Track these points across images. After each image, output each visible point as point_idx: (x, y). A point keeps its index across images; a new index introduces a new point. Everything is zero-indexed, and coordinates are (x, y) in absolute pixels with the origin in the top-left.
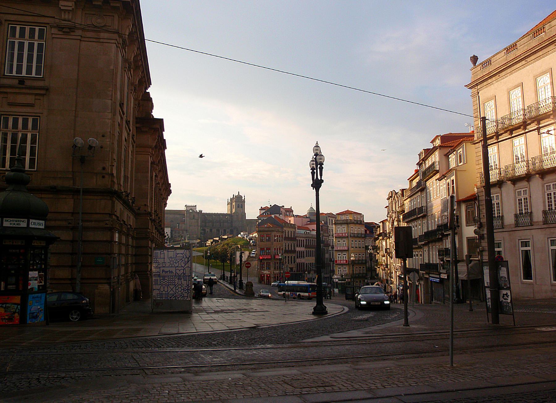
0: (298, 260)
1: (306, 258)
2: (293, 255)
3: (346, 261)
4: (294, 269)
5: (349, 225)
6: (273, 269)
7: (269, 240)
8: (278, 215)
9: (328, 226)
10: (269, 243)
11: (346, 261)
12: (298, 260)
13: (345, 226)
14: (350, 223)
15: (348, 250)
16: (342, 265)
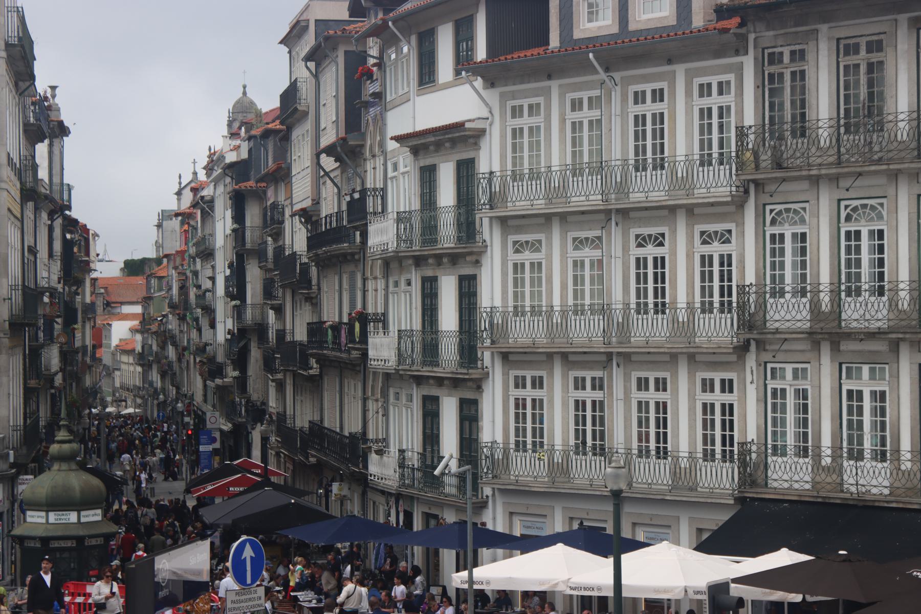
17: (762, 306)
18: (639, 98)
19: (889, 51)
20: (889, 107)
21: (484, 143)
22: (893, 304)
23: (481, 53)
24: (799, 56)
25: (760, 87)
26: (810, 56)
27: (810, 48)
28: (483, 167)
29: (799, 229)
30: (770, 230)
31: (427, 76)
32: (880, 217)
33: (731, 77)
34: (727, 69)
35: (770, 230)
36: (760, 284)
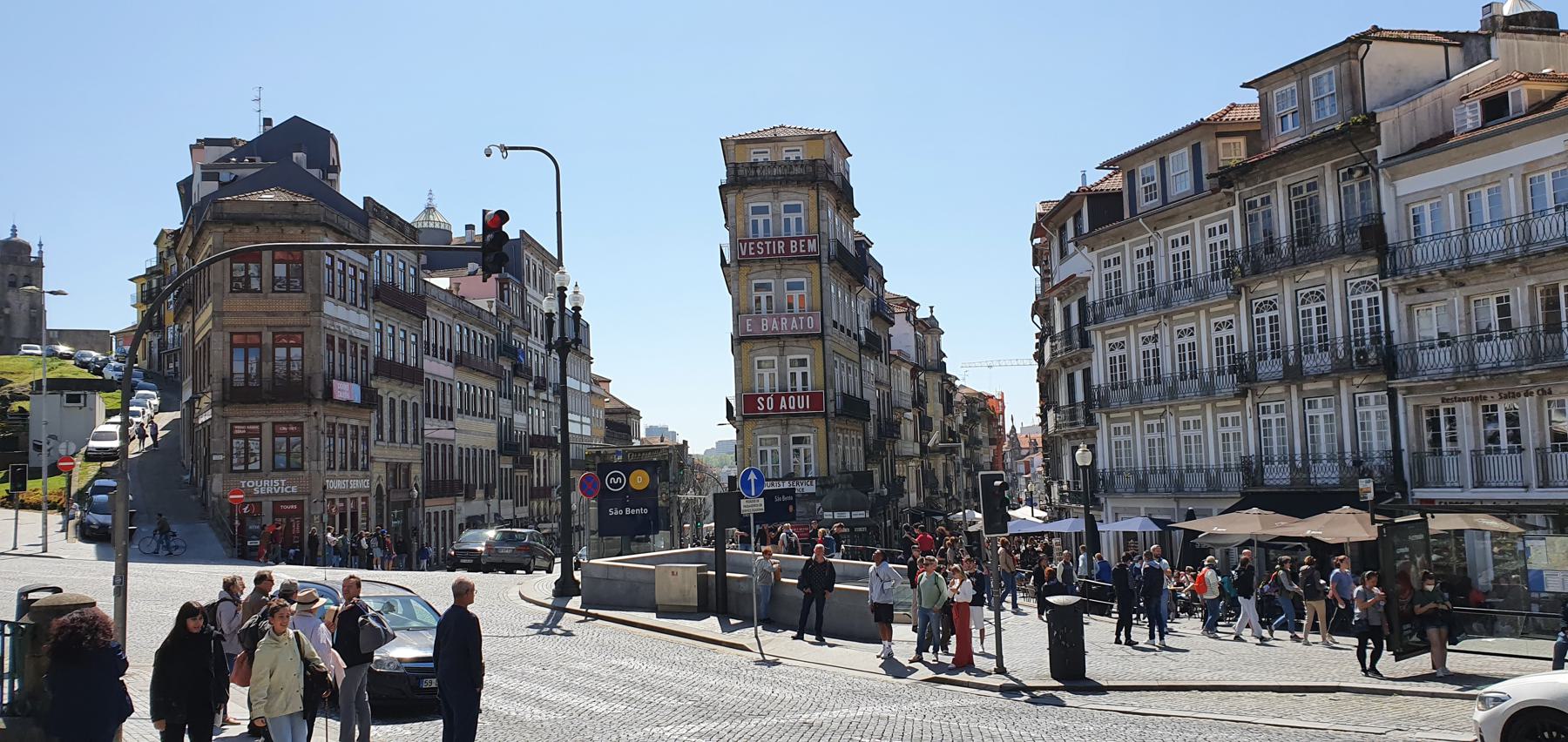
0: (435, 430)
1: (459, 421)
2: (412, 395)
3: (816, 399)
4: (416, 471)
5: (826, 195)
6: (323, 464)
7: (287, 286)
8: (315, 172)
9: (523, 290)
10: (295, 302)
11: (816, 399)
12: (435, 430)
13: (801, 197)
14: (831, 185)
15: (821, 336)
16: (786, 418)
17: (1253, 364)
18: (1175, 243)
19: (1321, 188)
20: (1324, 224)
21: (1090, 284)
22: (1334, 355)
23: (1086, 229)
24: (1266, 201)
25: (1244, 225)
26: (1273, 200)
27: (1272, 194)
28: (1090, 300)
29: (1273, 313)
30: (1256, 317)
31: (1063, 254)
32: (1322, 298)
33: (1226, 221)
34: (1223, 217)
35: (1256, 317)
36: (1252, 351)
